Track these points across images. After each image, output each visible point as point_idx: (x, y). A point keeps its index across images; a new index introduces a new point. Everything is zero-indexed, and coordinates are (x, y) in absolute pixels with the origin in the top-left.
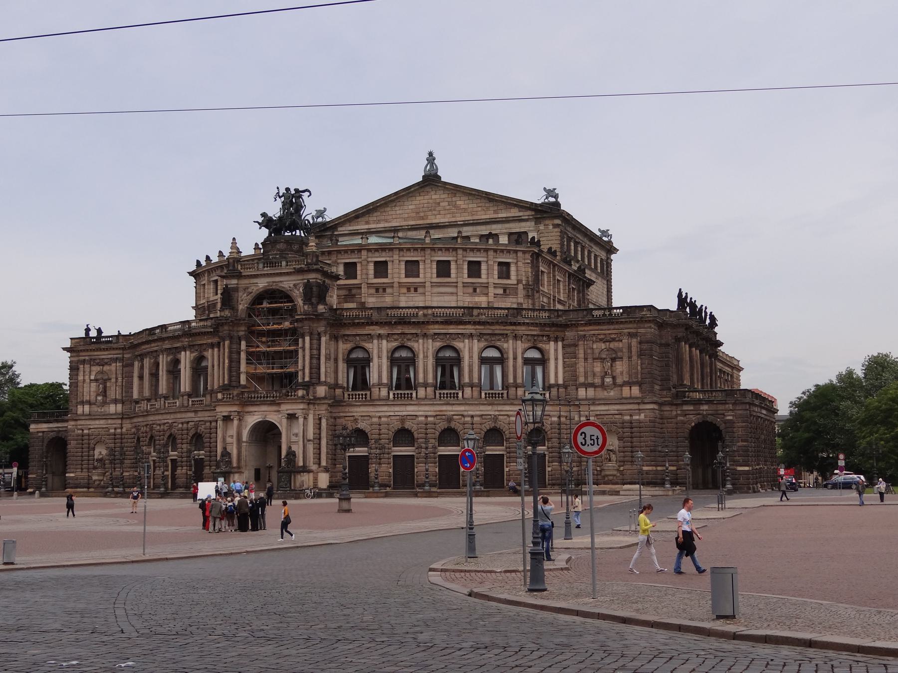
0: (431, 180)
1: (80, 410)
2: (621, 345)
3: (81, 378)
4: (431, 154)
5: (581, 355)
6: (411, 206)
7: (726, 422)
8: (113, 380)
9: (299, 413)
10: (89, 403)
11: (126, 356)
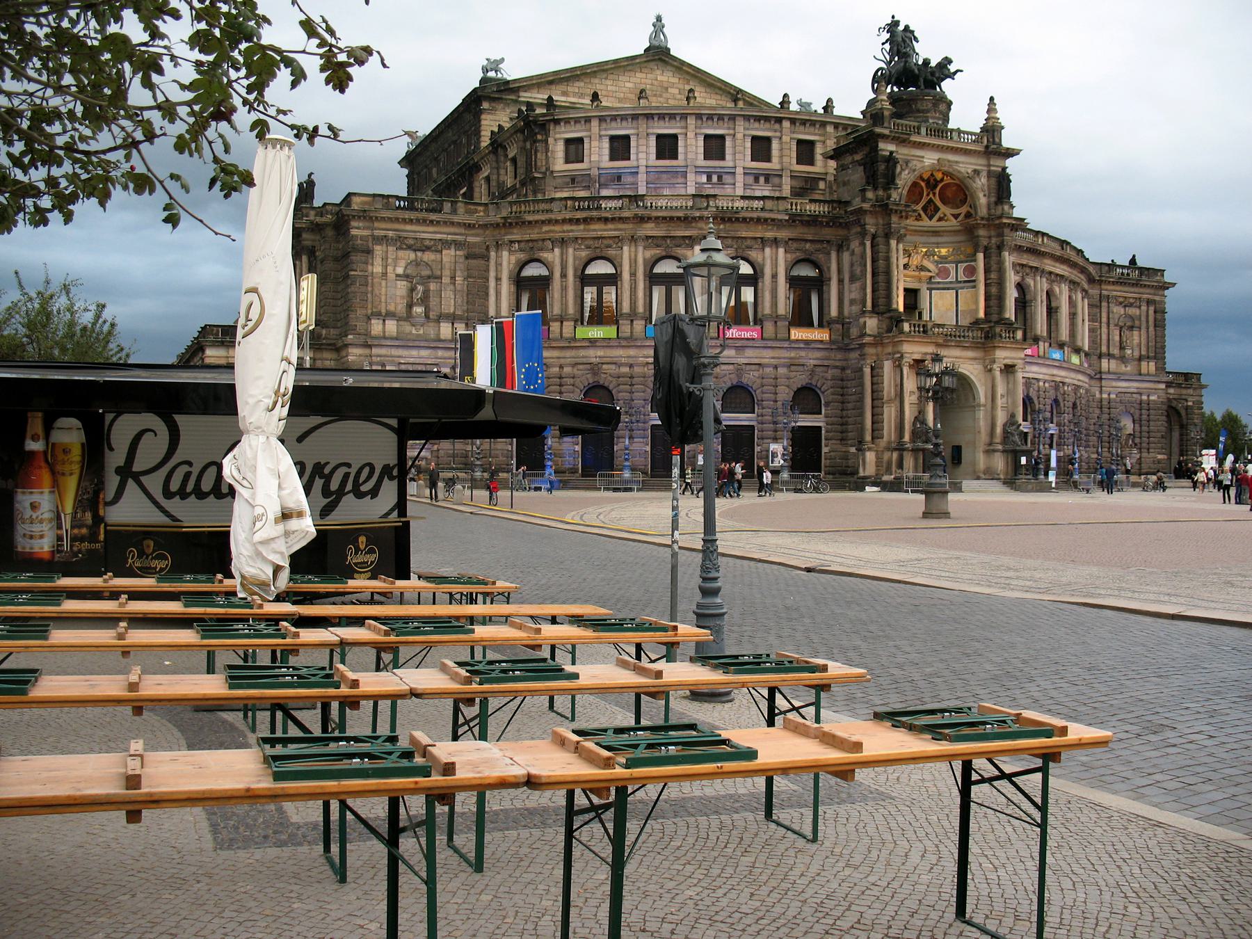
0: (658, 54)
1: (376, 327)
2: (1138, 312)
3: (378, 269)
4: (659, 19)
5: (1104, 319)
6: (629, 83)
7: (1187, 408)
8: (446, 280)
9: (1019, 363)
10: (390, 315)
11: (470, 239)
